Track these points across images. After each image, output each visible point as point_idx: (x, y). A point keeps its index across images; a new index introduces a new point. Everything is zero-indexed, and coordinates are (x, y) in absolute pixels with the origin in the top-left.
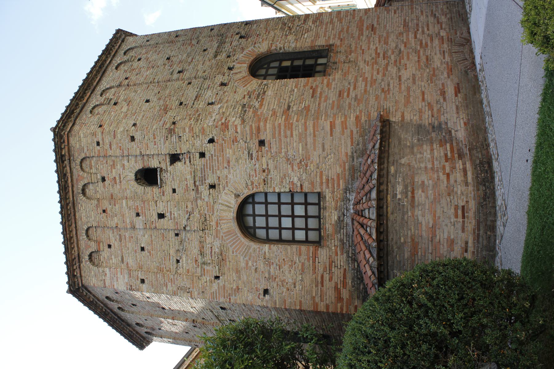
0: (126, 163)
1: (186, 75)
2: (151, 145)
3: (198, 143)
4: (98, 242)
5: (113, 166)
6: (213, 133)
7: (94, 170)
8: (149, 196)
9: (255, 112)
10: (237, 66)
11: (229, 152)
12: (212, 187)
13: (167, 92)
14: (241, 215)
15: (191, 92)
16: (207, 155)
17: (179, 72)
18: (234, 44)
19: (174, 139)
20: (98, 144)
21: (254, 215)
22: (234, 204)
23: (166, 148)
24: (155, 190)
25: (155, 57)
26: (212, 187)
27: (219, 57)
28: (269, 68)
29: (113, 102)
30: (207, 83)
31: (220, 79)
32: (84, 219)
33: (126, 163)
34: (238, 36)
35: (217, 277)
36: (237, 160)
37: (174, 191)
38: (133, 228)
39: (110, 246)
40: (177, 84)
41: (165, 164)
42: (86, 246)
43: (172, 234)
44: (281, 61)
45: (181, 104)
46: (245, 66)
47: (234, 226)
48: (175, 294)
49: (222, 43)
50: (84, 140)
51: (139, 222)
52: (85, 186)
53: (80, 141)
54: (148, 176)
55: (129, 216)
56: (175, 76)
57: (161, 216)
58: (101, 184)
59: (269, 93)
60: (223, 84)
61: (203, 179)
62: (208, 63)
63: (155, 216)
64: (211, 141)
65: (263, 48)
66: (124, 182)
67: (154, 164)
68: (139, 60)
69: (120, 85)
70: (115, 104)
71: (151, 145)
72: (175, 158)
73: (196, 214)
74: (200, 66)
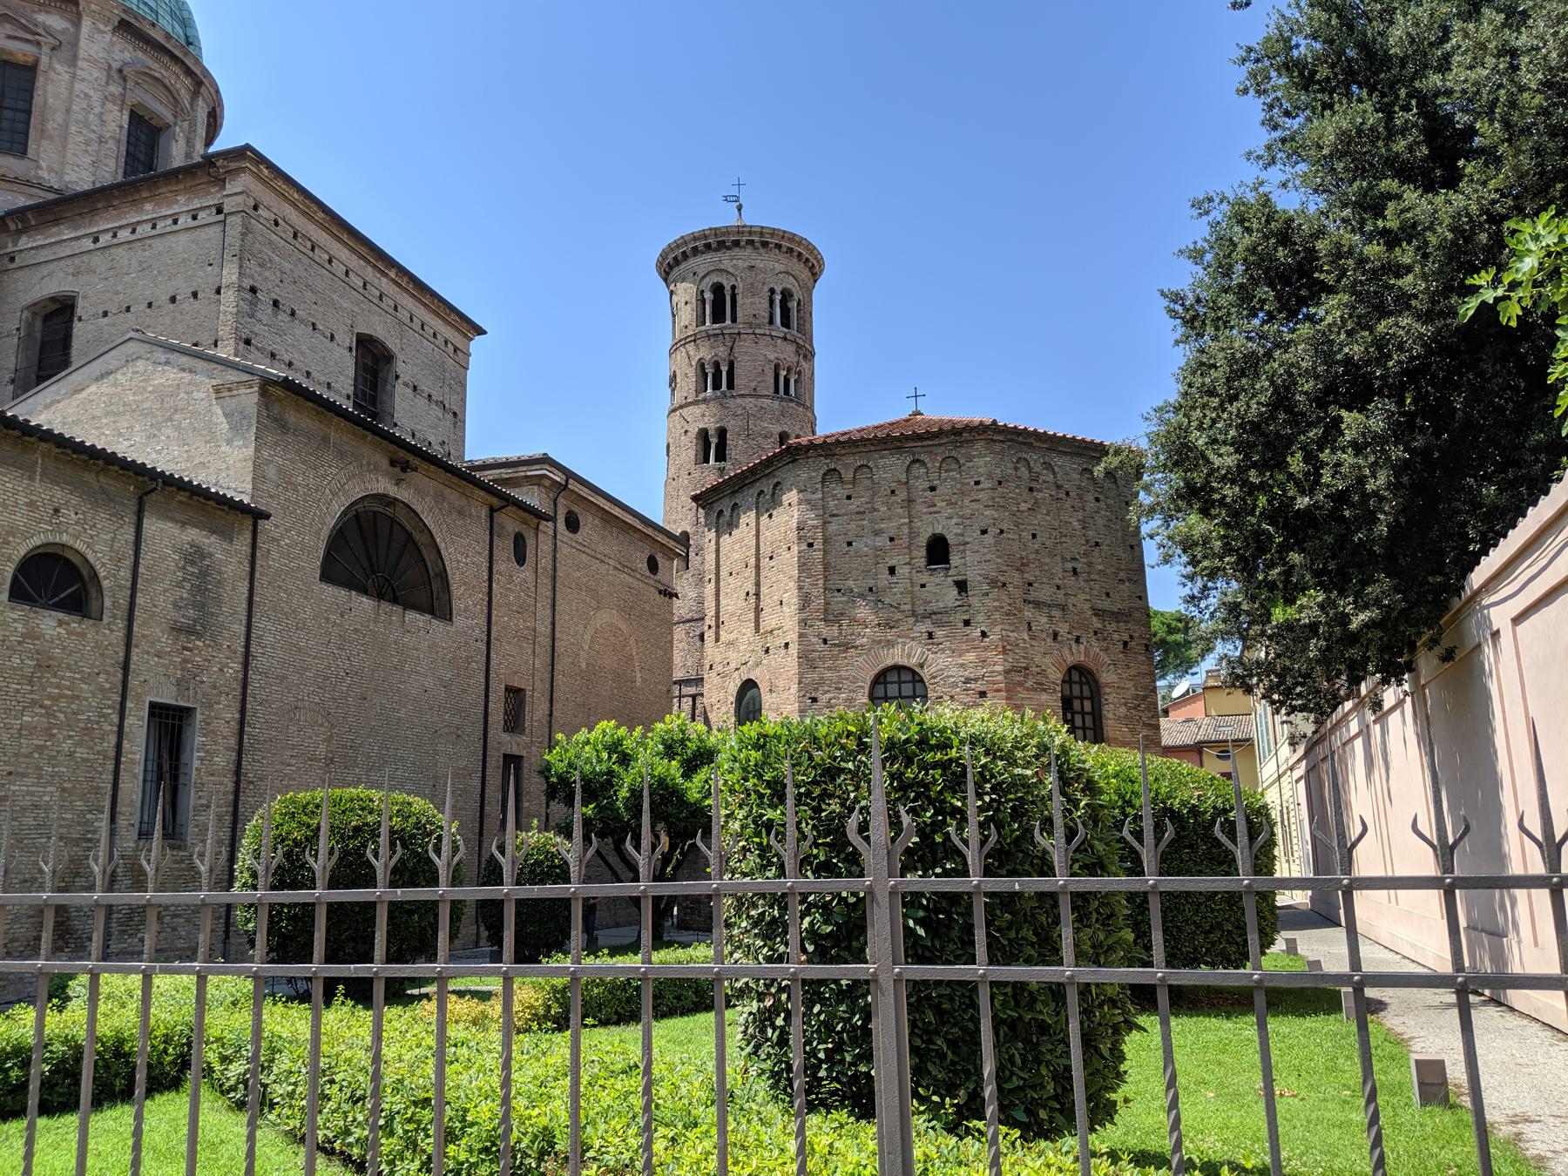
0: (954, 521)
1: (1071, 581)
2: (977, 557)
3: (980, 618)
4: (854, 482)
5: (950, 503)
6: (993, 637)
7: (944, 475)
8: (915, 553)
9: (1021, 684)
10: (1082, 647)
11: (971, 656)
12: (930, 636)
13: (1047, 560)
14: (898, 668)
15: (1044, 593)
16: (968, 630)
17: (1074, 570)
18: (1116, 636)
19: (985, 587)
20: (977, 483)
21: (900, 683)
22: (912, 662)
23: (973, 576)
24: (923, 562)
25: (1100, 522)
26: (930, 636)
27: (1094, 619)
28: (1081, 683)
29: (1033, 485)
30: (1056, 613)
31: (1063, 628)
32: (881, 462)
33: (954, 521)
34: (1126, 637)
35: (825, 641)
36: (962, 665)
37: (923, 586)
38: (877, 533)
39: (849, 497)
40: (1058, 571)
41: (954, 574)
42: (847, 464)
43: (871, 583)
44: (1091, 698)
45: (1030, 585)
46: (1080, 657)
47: (890, 662)
48: (800, 588)
49: (1117, 616)
50: (981, 462)
51: (882, 541)
52: (923, 463)
53: (980, 456)
54: (938, 551)
55: (890, 527)
56: (1069, 566)
57: (892, 570)
58: (927, 485)
59: (1044, 697)
60: (1055, 636)
61: (940, 625)
62: (1087, 606)
63: (892, 563)
64: (984, 634)
65: (1107, 677)
66: (930, 518)
67: (955, 560)
68: (1097, 500)
69: (1059, 487)
70: (1031, 489)
71: (977, 557)
72: (962, 586)
73: (898, 616)
74: (1082, 596)
